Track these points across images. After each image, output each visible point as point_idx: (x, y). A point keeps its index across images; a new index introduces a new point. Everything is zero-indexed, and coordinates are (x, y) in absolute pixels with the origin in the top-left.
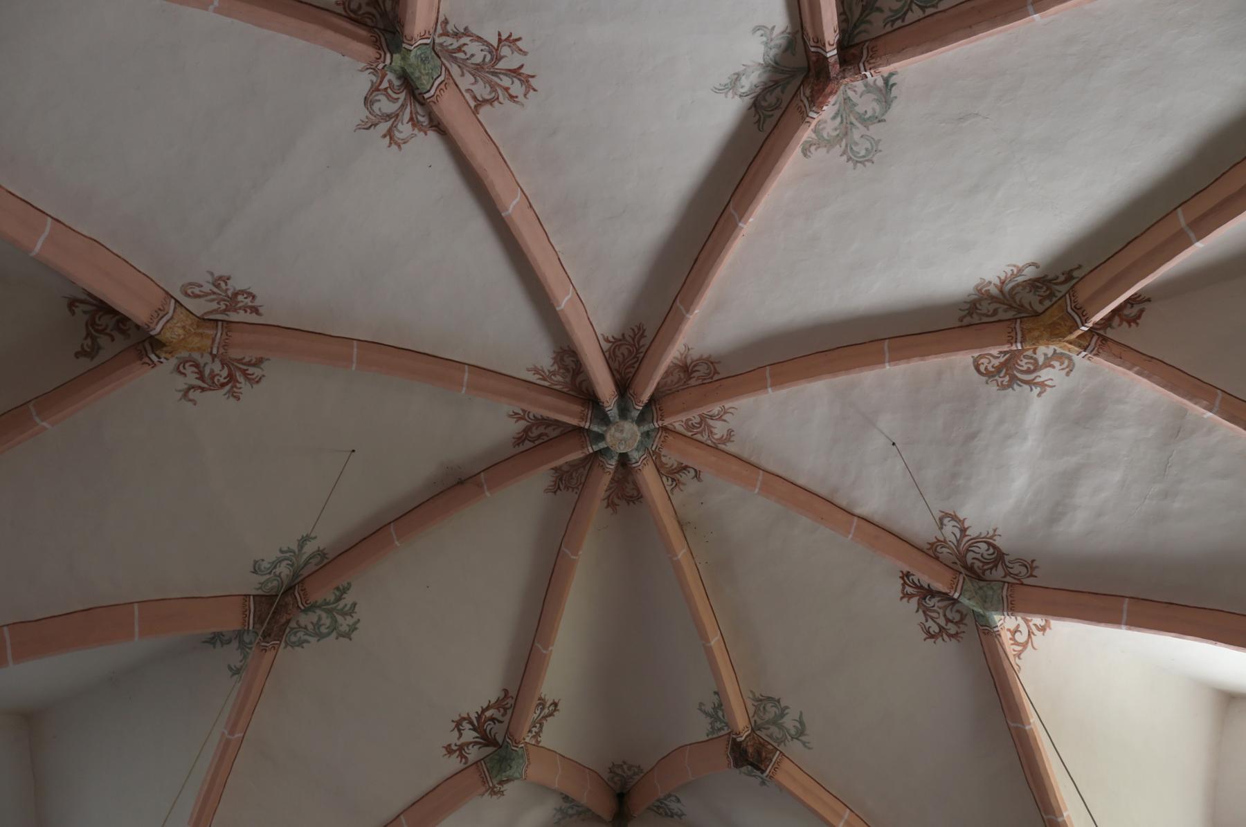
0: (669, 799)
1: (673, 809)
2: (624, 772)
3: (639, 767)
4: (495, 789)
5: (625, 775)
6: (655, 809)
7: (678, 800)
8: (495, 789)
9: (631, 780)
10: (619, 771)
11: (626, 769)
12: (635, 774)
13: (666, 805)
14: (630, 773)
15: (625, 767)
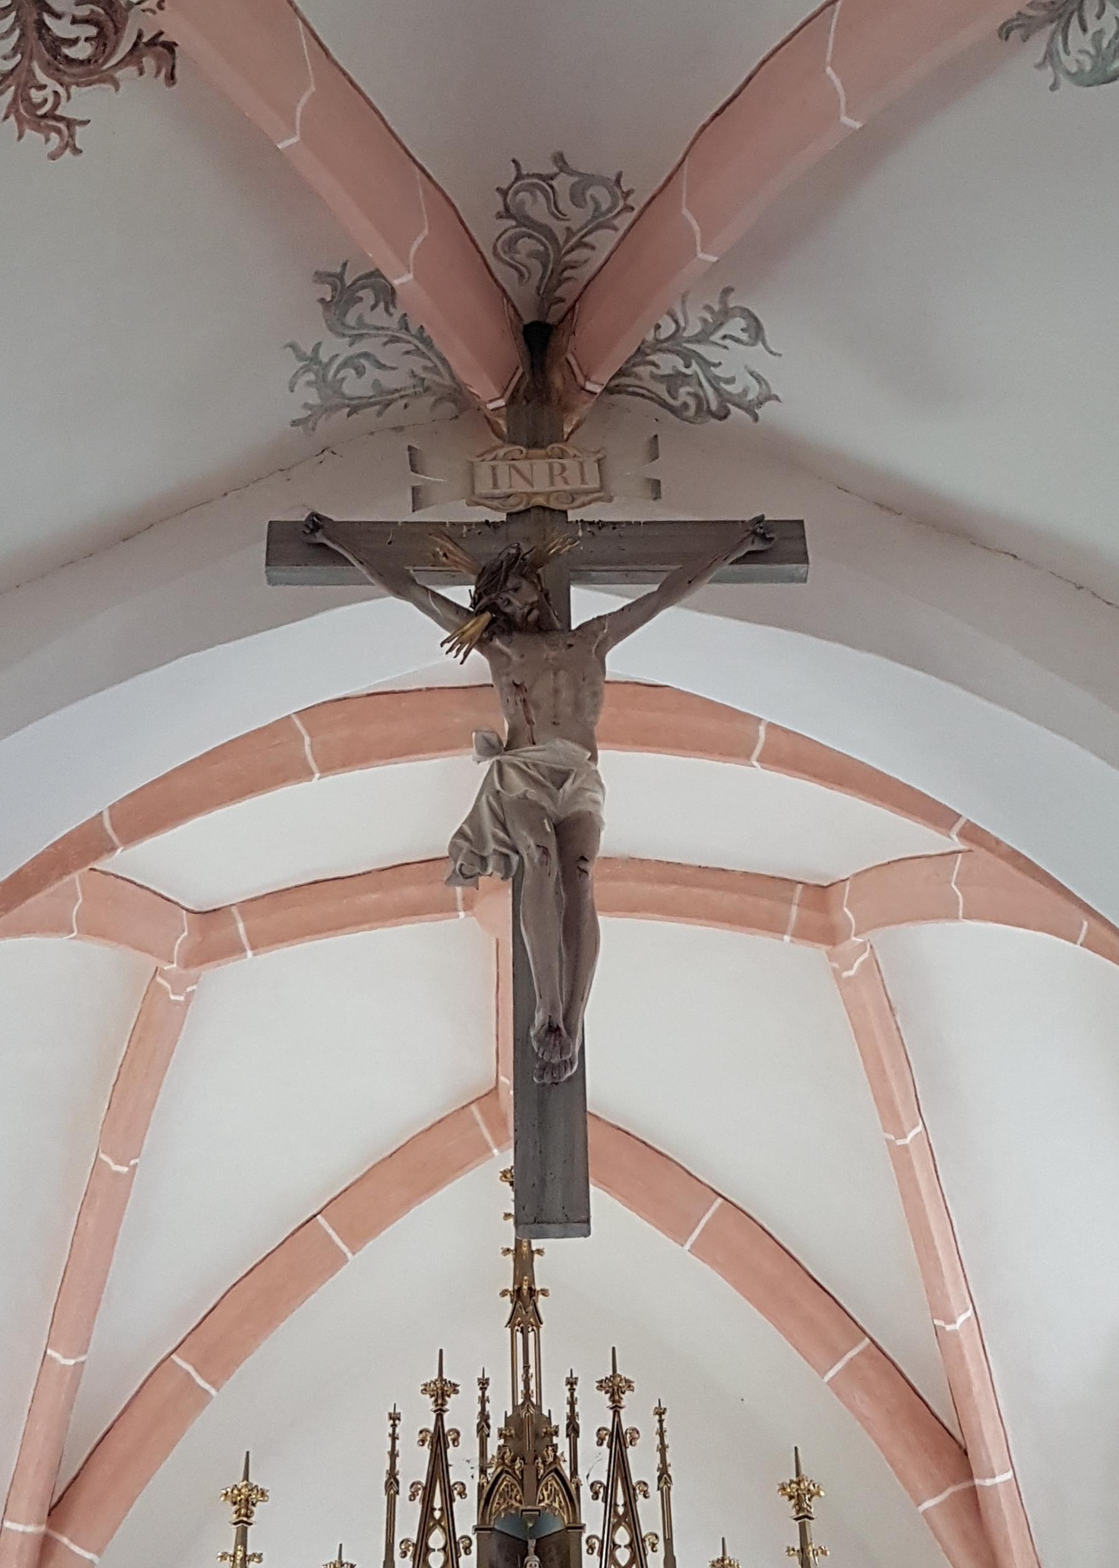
0: (716, 337)
1: (731, 381)
2: (558, 214)
3: (618, 181)
4: (36, 96)
5: (558, 228)
6: (661, 390)
7: (756, 331)
8: (36, 96)
9: (584, 253)
10: (537, 208)
11: (565, 204)
12: (600, 221)
13: (705, 363)
14: (578, 217)
15: (563, 183)
